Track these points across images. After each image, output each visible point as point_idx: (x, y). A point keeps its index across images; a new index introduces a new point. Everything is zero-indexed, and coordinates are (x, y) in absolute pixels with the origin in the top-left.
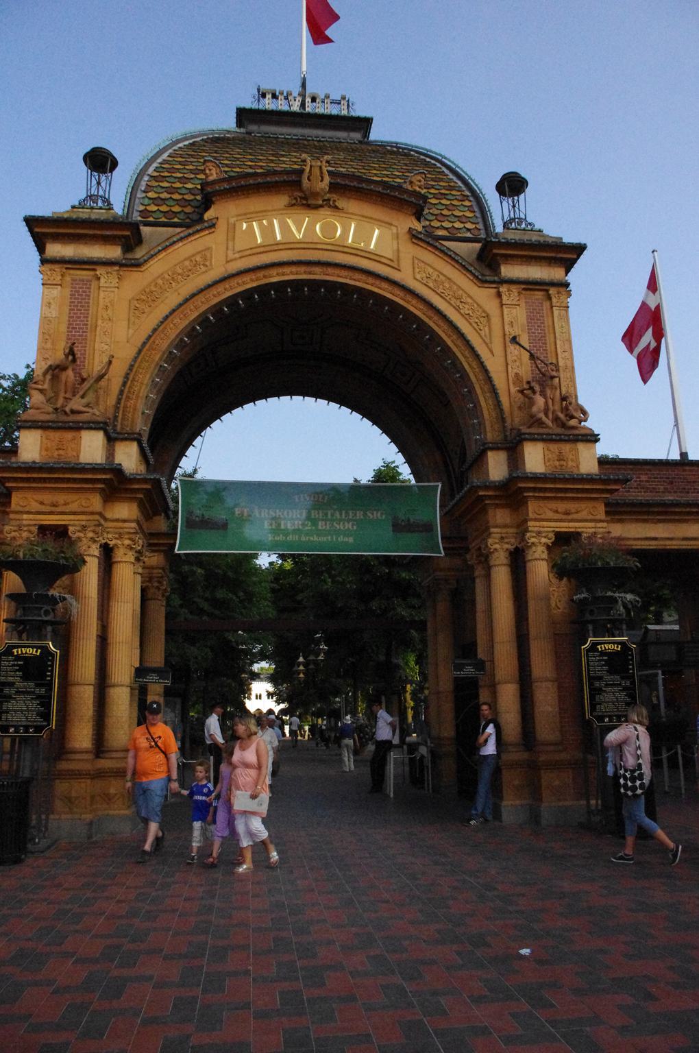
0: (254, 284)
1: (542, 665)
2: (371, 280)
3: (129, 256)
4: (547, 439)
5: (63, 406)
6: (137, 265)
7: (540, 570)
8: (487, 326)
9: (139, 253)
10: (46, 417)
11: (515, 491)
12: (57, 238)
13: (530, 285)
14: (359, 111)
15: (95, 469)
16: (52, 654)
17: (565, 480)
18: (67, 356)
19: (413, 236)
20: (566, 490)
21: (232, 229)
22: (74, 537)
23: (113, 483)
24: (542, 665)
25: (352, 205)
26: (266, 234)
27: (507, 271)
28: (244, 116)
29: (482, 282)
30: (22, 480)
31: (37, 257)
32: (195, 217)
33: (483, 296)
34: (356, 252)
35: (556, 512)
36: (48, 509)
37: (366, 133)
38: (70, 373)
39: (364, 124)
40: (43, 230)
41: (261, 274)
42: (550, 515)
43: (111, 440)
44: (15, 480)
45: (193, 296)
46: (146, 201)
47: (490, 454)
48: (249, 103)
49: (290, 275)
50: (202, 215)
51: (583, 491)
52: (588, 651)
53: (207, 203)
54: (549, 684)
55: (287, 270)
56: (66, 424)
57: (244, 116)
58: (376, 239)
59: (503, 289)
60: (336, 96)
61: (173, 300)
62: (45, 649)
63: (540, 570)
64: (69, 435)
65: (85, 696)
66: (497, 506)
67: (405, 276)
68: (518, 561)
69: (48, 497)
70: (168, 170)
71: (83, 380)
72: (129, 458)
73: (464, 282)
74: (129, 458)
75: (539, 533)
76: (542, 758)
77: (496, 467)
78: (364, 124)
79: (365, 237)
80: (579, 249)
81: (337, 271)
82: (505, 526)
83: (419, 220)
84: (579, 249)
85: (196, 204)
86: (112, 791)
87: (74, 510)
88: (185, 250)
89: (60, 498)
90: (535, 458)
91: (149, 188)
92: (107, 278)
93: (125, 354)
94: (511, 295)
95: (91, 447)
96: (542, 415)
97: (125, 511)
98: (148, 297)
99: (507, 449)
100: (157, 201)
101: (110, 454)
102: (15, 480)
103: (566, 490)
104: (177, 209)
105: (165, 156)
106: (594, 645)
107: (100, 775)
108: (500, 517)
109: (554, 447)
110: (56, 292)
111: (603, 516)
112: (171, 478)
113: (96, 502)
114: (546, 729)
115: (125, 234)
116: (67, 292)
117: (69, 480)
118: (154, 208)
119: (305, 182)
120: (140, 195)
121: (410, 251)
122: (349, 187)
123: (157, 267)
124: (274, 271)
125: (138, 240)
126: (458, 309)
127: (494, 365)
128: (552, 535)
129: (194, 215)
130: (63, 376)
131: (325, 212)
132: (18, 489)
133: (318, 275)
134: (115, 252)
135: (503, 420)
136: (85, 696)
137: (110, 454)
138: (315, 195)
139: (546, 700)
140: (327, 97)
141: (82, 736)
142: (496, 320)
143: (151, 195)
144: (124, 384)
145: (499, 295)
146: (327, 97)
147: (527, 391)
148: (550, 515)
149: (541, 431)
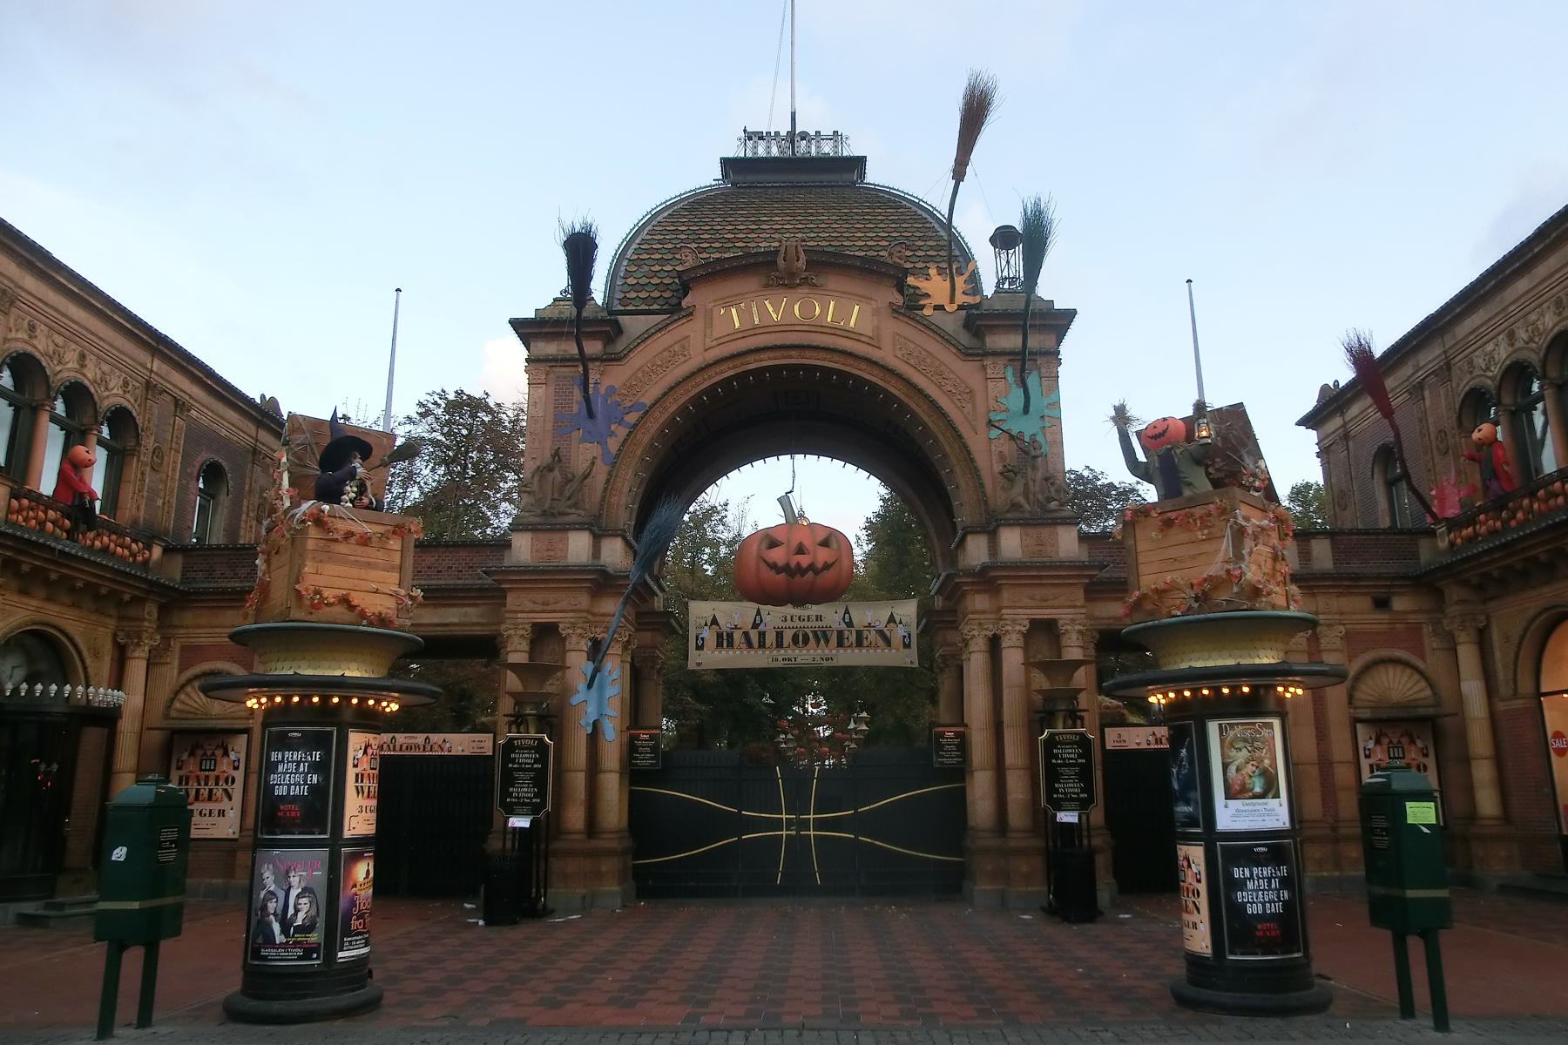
0: (732, 373)
1: (1014, 753)
2: (850, 361)
3: (610, 349)
4: (1023, 523)
5: (551, 507)
6: (617, 359)
7: (1013, 659)
8: (972, 401)
9: (620, 346)
10: (537, 520)
11: (989, 578)
12: (537, 336)
14: (852, 150)
15: (582, 569)
16: (547, 746)
17: (1043, 566)
18: (553, 457)
19: (895, 310)
20: (1041, 577)
21: (709, 317)
22: (564, 633)
23: (601, 581)
25: (833, 282)
26: (745, 320)
28: (727, 163)
29: (966, 354)
30: (516, 581)
31: (524, 353)
32: (674, 301)
33: (966, 371)
34: (835, 331)
35: (1032, 598)
36: (540, 608)
37: (862, 174)
38: (556, 473)
39: (859, 163)
40: (525, 329)
41: (738, 362)
42: (1026, 601)
43: (597, 538)
44: (511, 581)
45: (672, 388)
46: (626, 288)
47: (969, 538)
48: (734, 150)
49: (767, 361)
50: (680, 299)
51: (1059, 577)
52: (1046, 741)
53: (685, 289)
54: (1021, 772)
55: (764, 356)
57: (727, 163)
58: (855, 317)
59: (988, 362)
60: (827, 131)
62: (541, 740)
63: (1013, 659)
64: (556, 537)
65: (578, 781)
66: (978, 592)
67: (887, 355)
68: (994, 644)
69: (540, 597)
70: (647, 251)
71: (569, 481)
72: (615, 554)
73: (946, 356)
74: (615, 554)
75: (1014, 621)
76: (1013, 844)
77: (976, 551)
78: (859, 163)
79: (844, 315)
80: (1070, 315)
81: (814, 354)
82: (984, 612)
83: (901, 292)
84: (1070, 315)
85: (674, 287)
86: (604, 869)
87: (565, 608)
89: (551, 596)
91: (628, 274)
94: (995, 367)
95: (578, 546)
96: (1021, 500)
97: (611, 606)
99: (988, 533)
100: (637, 287)
101: (596, 552)
102: (511, 581)
103: (1041, 577)
104: (656, 294)
105: (643, 235)
106: (1052, 735)
107: (594, 854)
108: (979, 602)
109: (1033, 531)
110: (541, 390)
111: (1080, 602)
112: (685, 510)
113: (584, 600)
115: (607, 326)
116: (552, 389)
117: (558, 581)
118: (633, 295)
119: (781, 262)
120: (619, 282)
121: (892, 328)
122: (825, 265)
123: (637, 360)
124: (751, 358)
125: (619, 331)
126: (940, 386)
127: (976, 443)
128: (1026, 623)
130: (550, 476)
131: (804, 290)
132: (511, 589)
133: (795, 359)
135: (986, 503)
136: (578, 781)
137: (596, 552)
138: (792, 275)
140: (818, 133)
141: (575, 817)
142: (979, 396)
143: (630, 281)
144: (608, 481)
145: (984, 368)
146: (818, 133)
147: (1009, 474)
148: (1026, 601)
149: (1018, 515)
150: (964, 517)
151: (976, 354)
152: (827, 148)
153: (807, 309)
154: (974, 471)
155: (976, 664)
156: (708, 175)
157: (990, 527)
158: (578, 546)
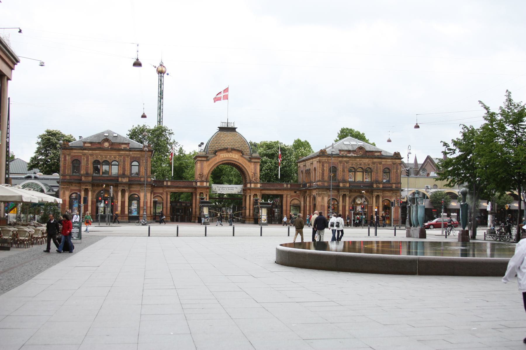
1: (251, 208)
11: (250, 189)
13: (255, 162)
19: (241, 156)
24: (251, 208)
27: (253, 160)
56: (202, 182)
61: (213, 165)
63: (252, 198)
67: (240, 161)
68: (250, 196)
73: (247, 162)
88: (214, 159)
90: (253, 186)
92: (205, 162)
93: (208, 172)
94: (252, 164)
95: (205, 184)
98: (209, 165)
108: (249, 191)
114: (251, 215)
121: (241, 158)
123: (211, 161)
127: (249, 173)
129: (215, 152)
134: (205, 159)
139: (251, 212)
150: (248, 181)
151: (250, 161)
152: (232, 125)
153: (231, 155)
154: (249, 176)
155: (248, 198)
156: (216, 130)
157: (251, 183)
158: (205, 184)
